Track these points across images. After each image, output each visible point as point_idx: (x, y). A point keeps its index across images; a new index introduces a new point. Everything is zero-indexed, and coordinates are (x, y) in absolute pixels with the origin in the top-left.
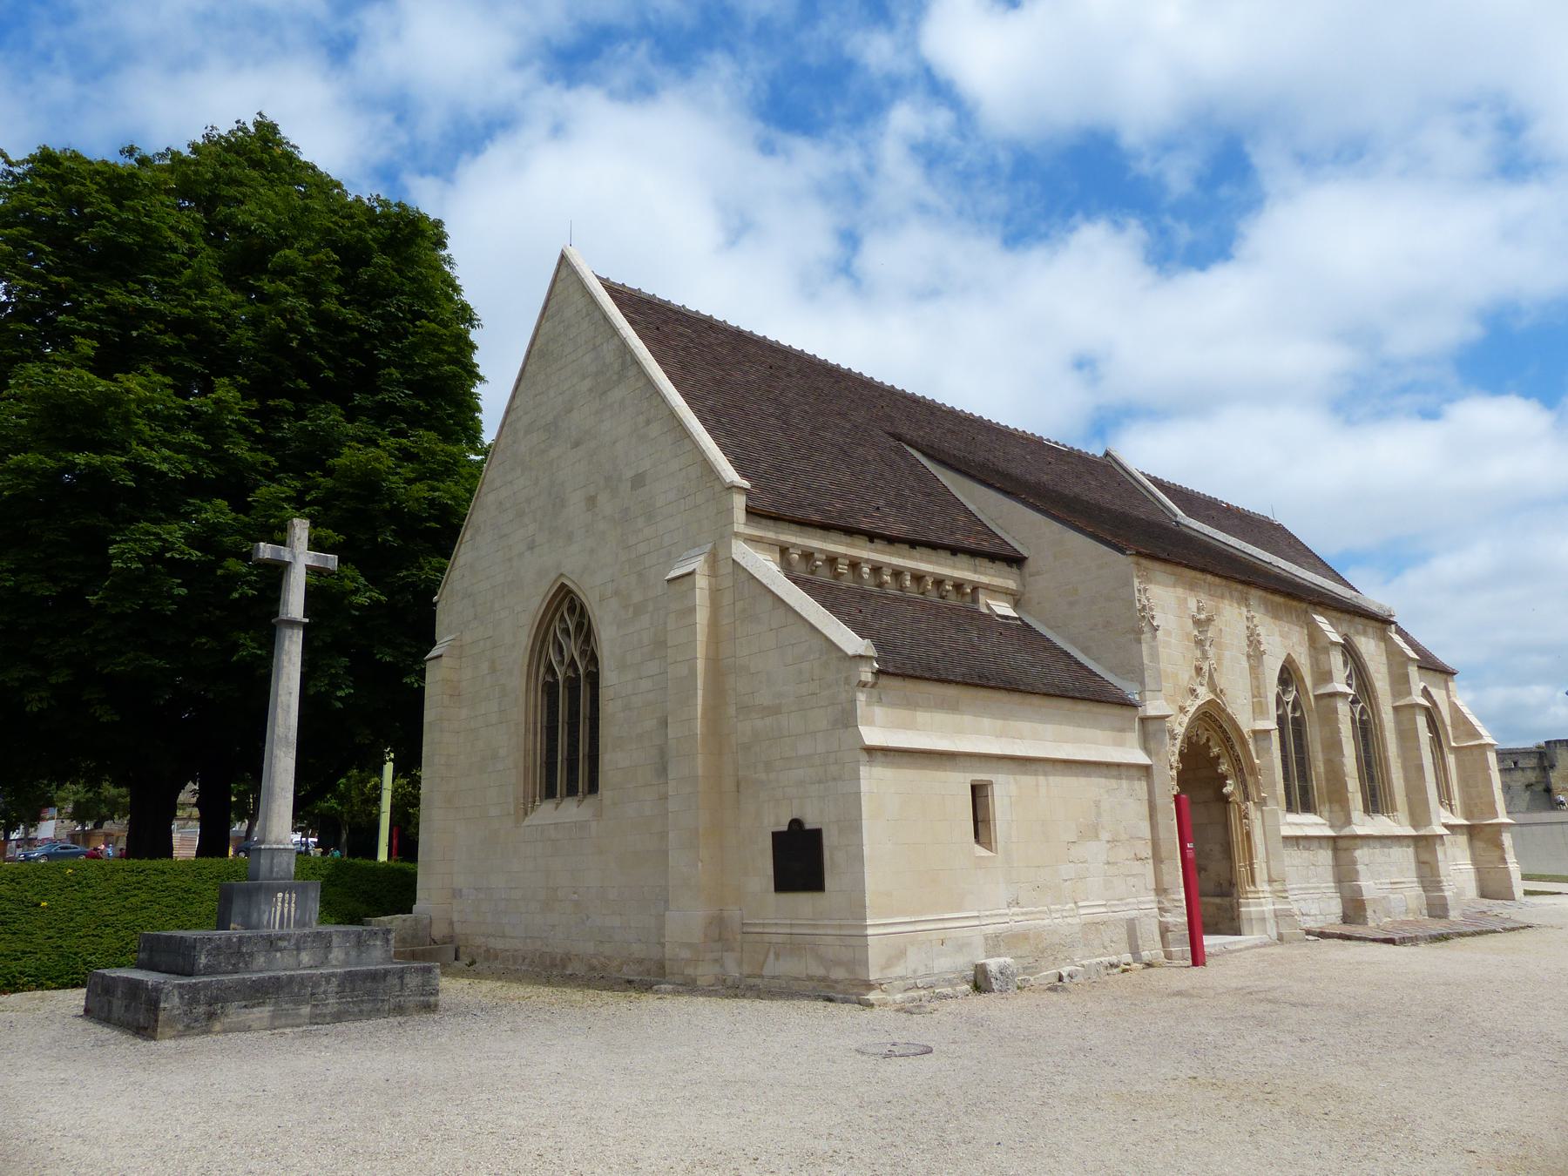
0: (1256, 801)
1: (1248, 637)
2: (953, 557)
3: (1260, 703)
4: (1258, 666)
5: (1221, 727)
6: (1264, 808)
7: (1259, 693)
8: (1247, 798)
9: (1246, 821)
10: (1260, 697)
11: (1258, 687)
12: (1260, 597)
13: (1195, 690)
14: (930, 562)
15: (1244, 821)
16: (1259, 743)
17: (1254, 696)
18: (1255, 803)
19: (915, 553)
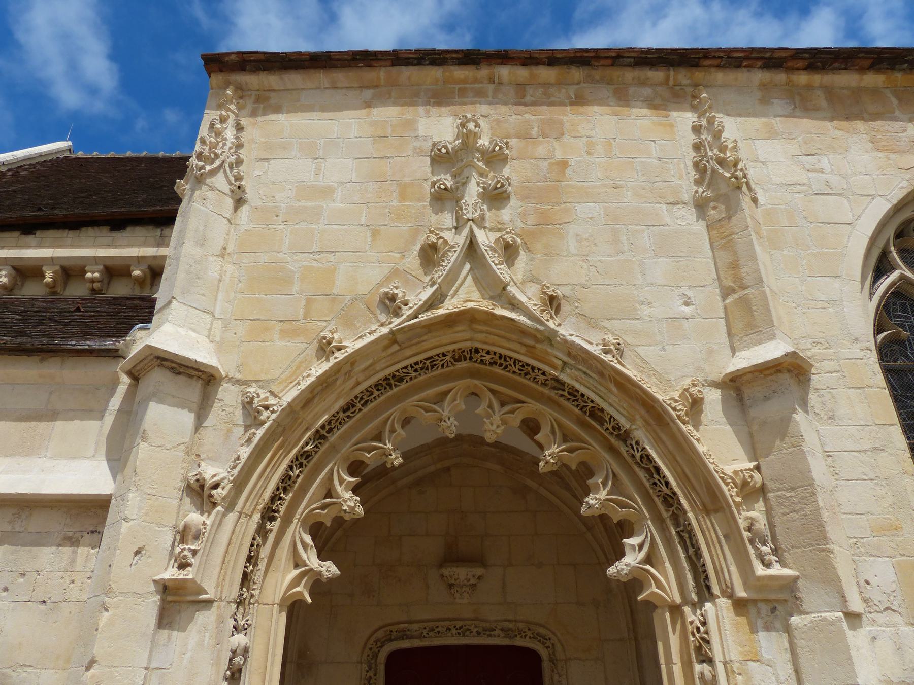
0: (741, 593)
1: (696, 165)
2: (114, 234)
3: (745, 304)
4: (729, 218)
5: (559, 384)
6: (795, 620)
7: (738, 279)
8: (705, 592)
9: (706, 667)
10: (744, 287)
11: (735, 266)
12: (763, 86)
13: (393, 298)
14: (72, 246)
15: (698, 667)
16: (753, 413)
17: (726, 292)
18: (740, 606)
19: (30, 239)
